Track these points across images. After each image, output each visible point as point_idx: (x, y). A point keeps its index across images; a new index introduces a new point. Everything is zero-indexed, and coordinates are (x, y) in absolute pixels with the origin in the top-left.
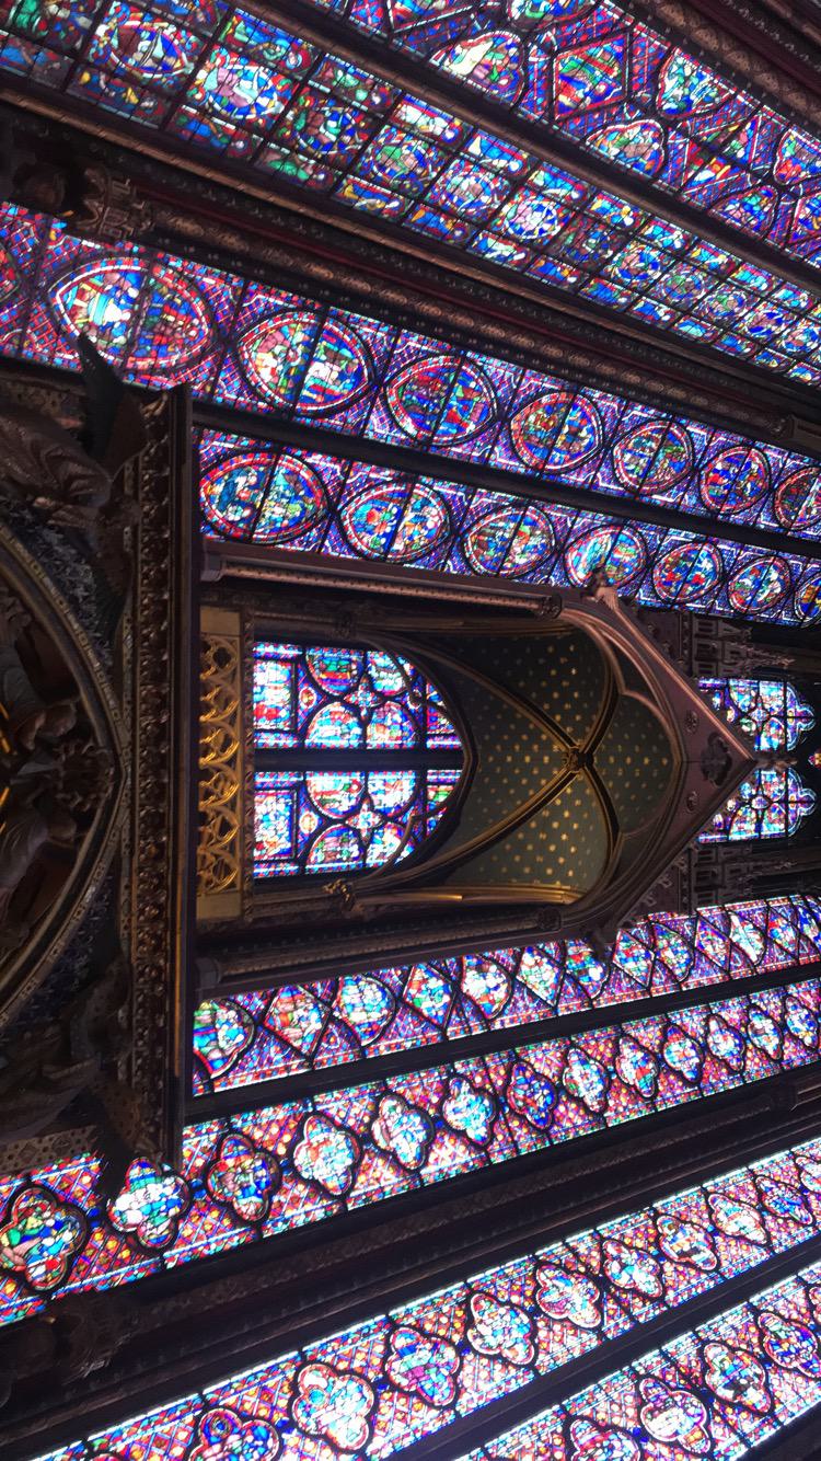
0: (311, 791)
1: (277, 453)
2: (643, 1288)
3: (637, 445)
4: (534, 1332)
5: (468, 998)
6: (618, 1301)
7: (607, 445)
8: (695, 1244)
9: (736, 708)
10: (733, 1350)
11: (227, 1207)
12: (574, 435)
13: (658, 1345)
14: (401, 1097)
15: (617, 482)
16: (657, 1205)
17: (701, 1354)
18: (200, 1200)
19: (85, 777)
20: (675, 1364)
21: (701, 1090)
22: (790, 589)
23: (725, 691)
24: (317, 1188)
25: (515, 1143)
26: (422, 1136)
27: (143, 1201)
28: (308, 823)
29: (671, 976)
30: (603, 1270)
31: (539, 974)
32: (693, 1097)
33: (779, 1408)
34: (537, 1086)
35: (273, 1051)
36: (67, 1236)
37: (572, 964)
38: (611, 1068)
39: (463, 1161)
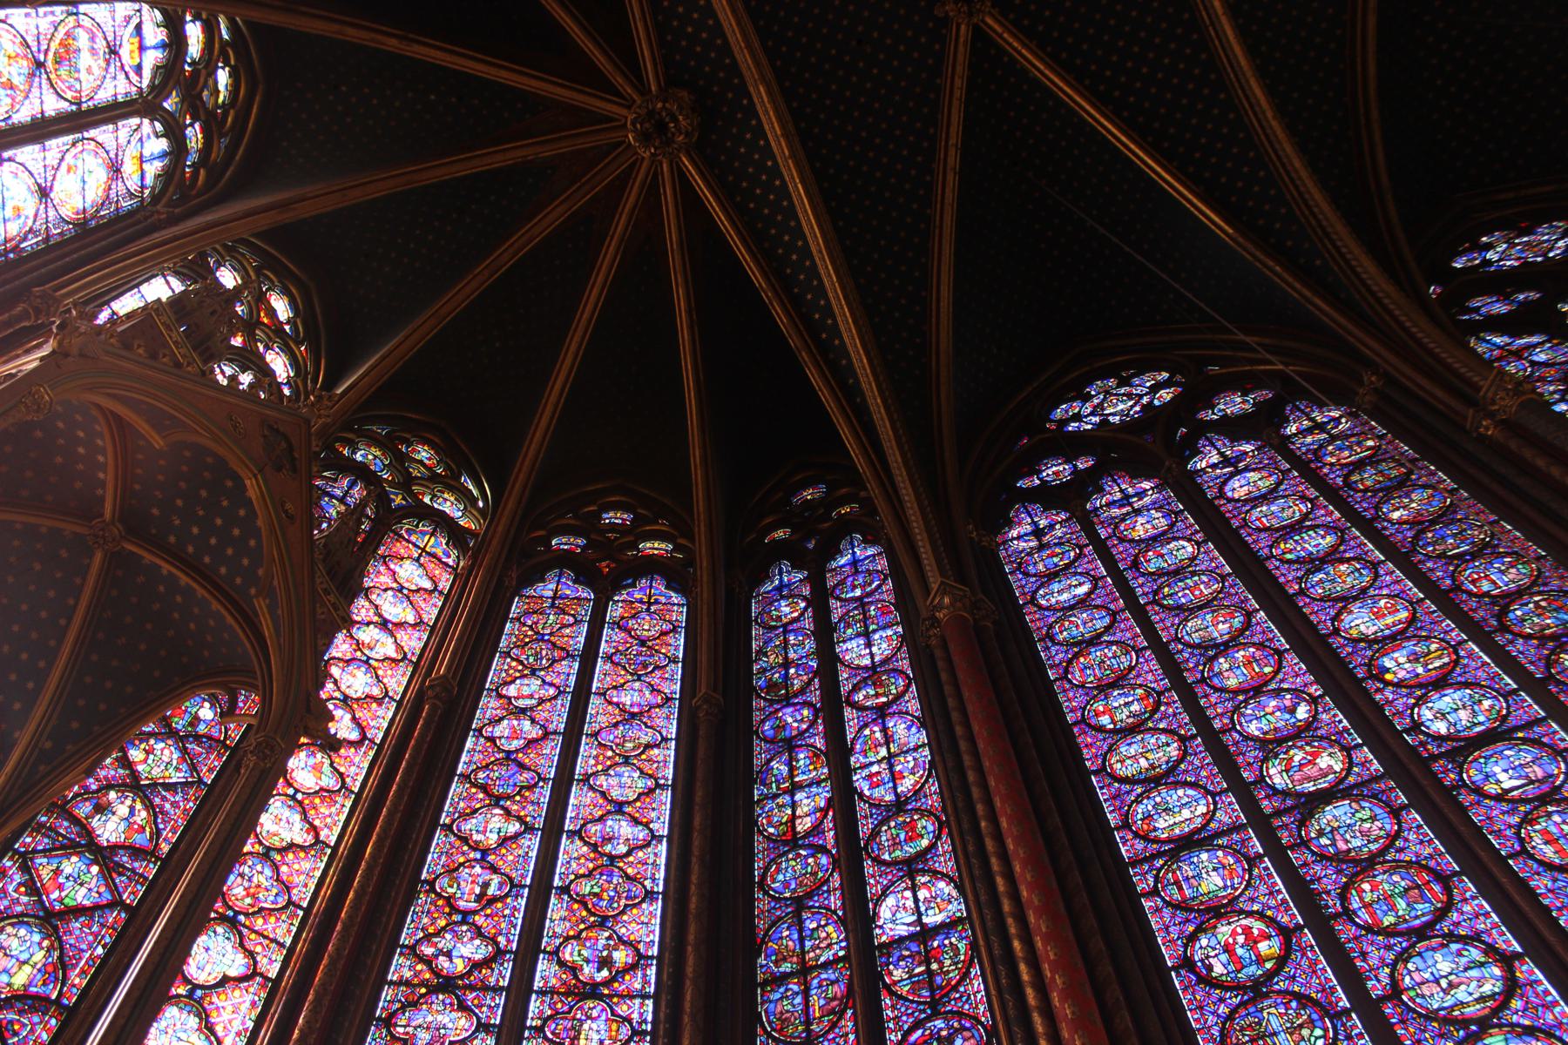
2: (478, 957)
5: (114, 848)
6: (472, 988)
8: (481, 880)
10: (577, 937)
13: (530, 991)
16: (424, 875)
17: (561, 963)
20: (553, 991)
21: (372, 741)
22: (115, 169)
25: (272, 941)
26: (193, 1021)
30: (436, 973)
31: (157, 760)
32: (372, 753)
33: (641, 947)
34: (247, 870)
37: (179, 723)
38: (291, 791)
39: (248, 1004)
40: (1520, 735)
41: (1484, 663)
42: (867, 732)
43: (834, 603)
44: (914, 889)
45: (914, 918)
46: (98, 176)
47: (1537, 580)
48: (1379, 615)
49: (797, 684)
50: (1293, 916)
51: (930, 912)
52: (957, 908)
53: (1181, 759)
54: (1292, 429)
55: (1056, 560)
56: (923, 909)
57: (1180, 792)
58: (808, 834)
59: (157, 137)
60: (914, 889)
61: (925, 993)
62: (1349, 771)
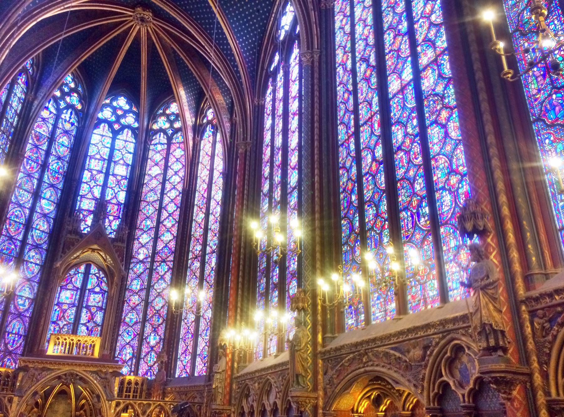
0: (90, 288)
1: (15, 295)
3: (21, 196)
4: (196, 276)
5: (143, 260)
7: (20, 206)
9: (97, 154)
11: (159, 325)
12: (17, 216)
14: (155, 283)
15: (29, 201)
18: (157, 329)
19: (72, 374)
22: (66, 132)
23: (91, 157)
24: (162, 307)
27: (153, 340)
28: (97, 289)
29: (155, 201)
35: (138, 308)
36: (153, 354)
37: (145, 229)
46: (64, 140)
59: (66, 113)
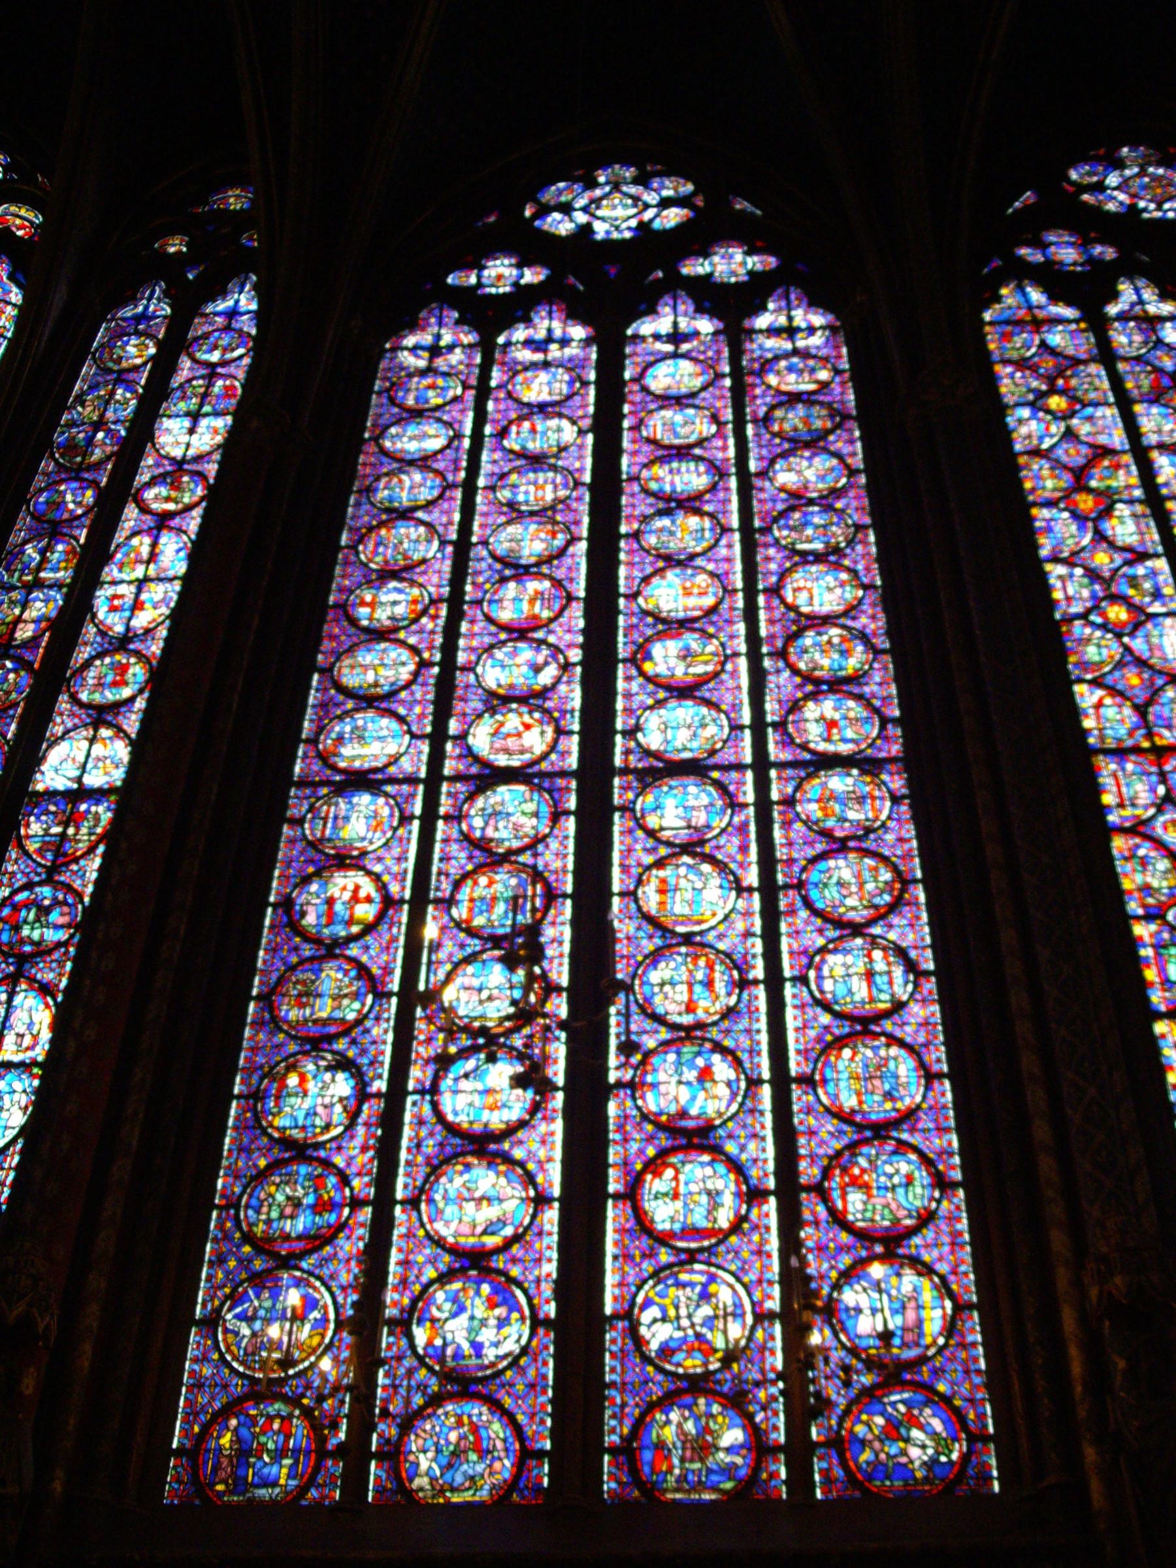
40: (715, 775)
41: (739, 687)
42: (135, 541)
43: (186, 363)
44: (92, 741)
45: (77, 773)
47: (851, 610)
48: (687, 593)
49: (97, 454)
50: (403, 888)
51: (94, 771)
52: (118, 776)
53: (407, 685)
54: (762, 321)
55: (431, 393)
56: (89, 766)
57: (385, 722)
58: (18, 647)
60: (92, 741)
61: (49, 856)
62: (544, 756)
